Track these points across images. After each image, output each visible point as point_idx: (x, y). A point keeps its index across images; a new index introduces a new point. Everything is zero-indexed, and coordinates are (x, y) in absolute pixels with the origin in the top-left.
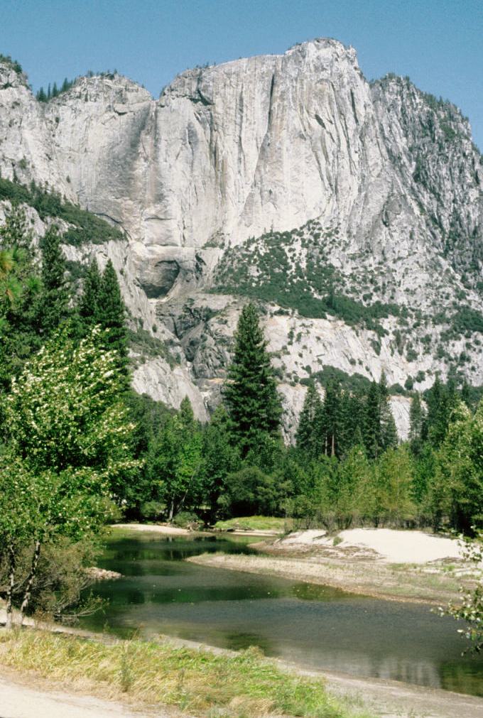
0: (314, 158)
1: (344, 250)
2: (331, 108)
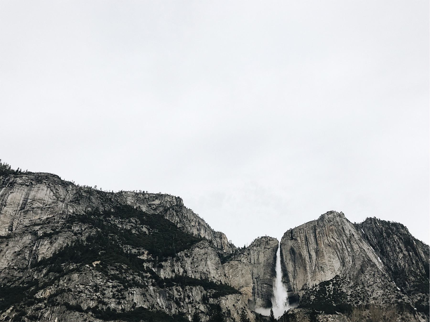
0: (335, 253)
1: (347, 285)
2: (337, 234)
